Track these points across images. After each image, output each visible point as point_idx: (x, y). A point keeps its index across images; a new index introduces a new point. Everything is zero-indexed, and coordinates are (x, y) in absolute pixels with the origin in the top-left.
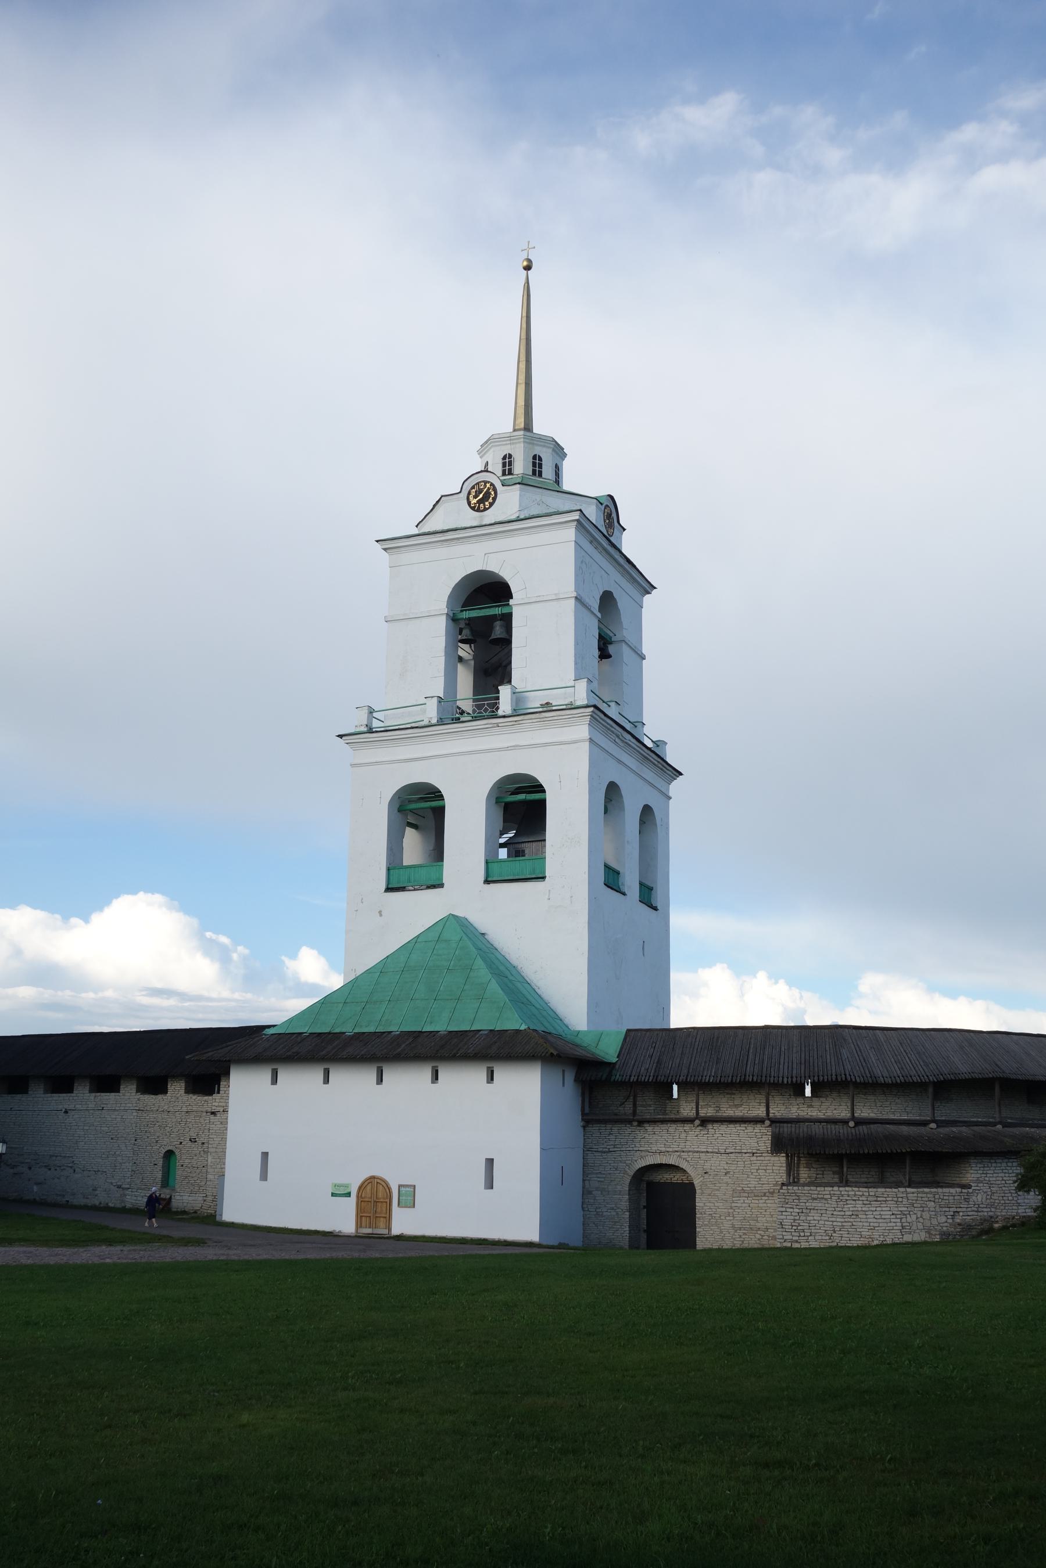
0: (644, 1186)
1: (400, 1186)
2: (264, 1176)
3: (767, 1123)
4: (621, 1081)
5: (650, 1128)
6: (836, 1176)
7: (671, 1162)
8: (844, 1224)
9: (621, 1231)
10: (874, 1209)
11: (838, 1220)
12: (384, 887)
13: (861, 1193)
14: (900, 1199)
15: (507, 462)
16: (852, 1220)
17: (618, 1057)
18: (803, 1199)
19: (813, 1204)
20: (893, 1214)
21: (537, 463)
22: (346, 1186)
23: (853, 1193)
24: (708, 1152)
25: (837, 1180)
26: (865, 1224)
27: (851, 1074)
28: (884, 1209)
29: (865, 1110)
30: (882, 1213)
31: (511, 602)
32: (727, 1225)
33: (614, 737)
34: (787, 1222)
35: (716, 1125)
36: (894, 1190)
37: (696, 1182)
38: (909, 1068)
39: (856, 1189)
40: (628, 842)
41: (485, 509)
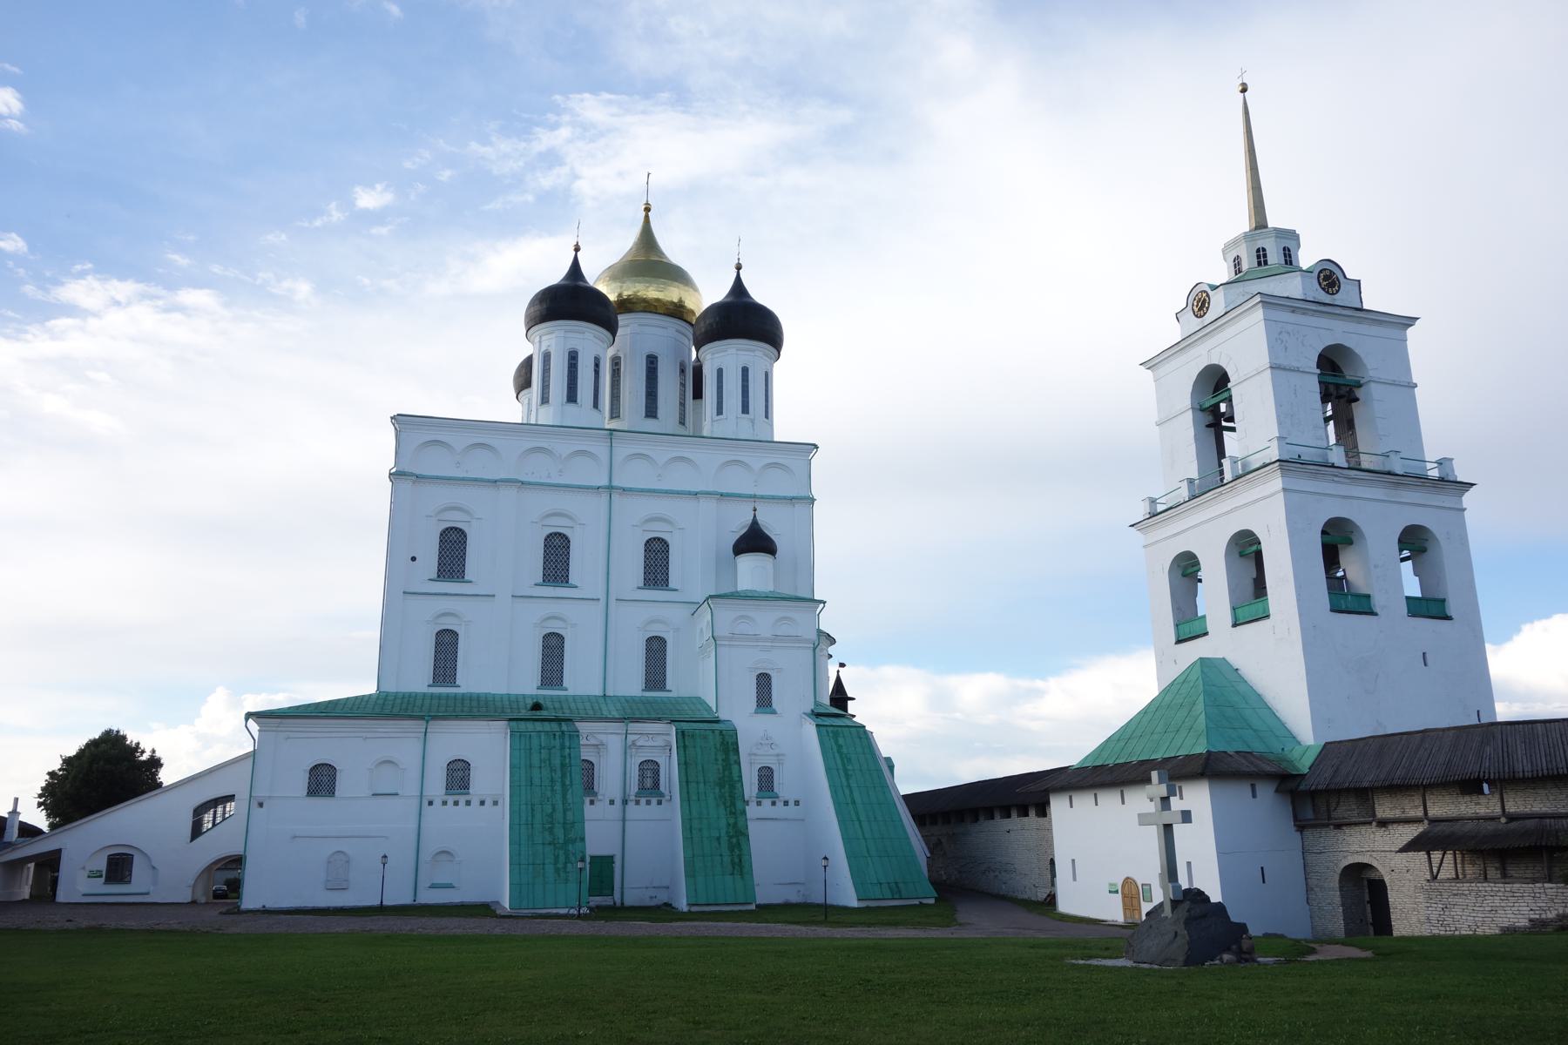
0: (1366, 883)
1: (1142, 885)
2: (1075, 879)
3: (1426, 822)
4: (1445, 782)
5: (1347, 830)
6: (1499, 872)
7: (1365, 861)
8: (1485, 919)
9: (1337, 926)
10: (1512, 905)
11: (1479, 915)
12: (1174, 641)
13: (1497, 889)
14: (1538, 895)
15: (1237, 262)
16: (1492, 916)
17: (1310, 768)
18: (1445, 895)
19: (1457, 900)
20: (1531, 910)
21: (1261, 256)
22: (1115, 885)
23: (1490, 889)
24: (1391, 851)
25: (1499, 876)
26: (1505, 919)
27: (1487, 771)
28: (1521, 904)
29: (1517, 804)
30: (1520, 908)
31: (1230, 385)
32: (1414, 919)
33: (1331, 478)
34: (1433, 917)
35: (1395, 826)
36: (1530, 885)
37: (1387, 879)
38: (1558, 759)
39: (1492, 885)
40: (1376, 566)
41: (1205, 314)
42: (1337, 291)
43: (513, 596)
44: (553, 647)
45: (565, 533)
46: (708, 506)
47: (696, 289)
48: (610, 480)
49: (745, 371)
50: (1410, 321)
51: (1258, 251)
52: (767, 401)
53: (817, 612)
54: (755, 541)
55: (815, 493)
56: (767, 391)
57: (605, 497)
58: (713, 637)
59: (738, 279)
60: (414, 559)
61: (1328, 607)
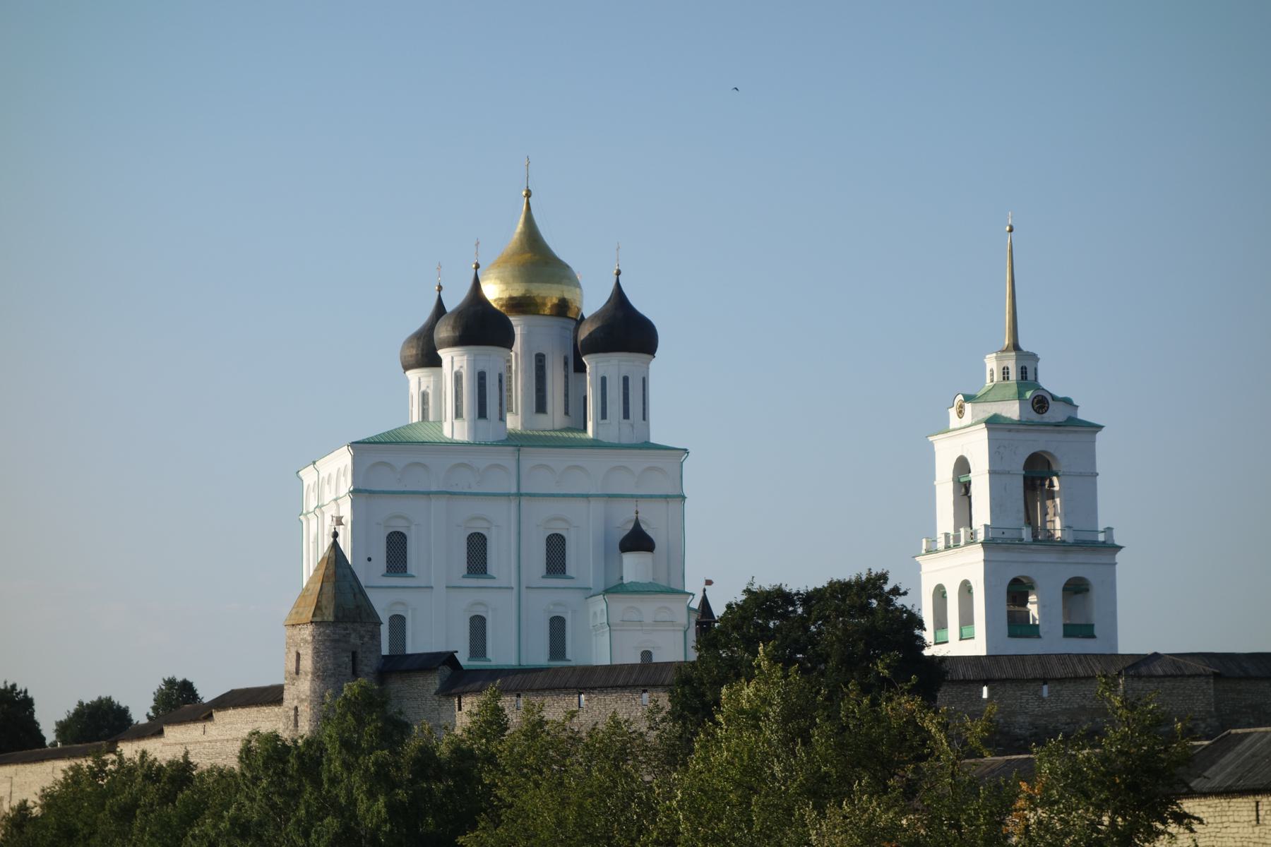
42: (1046, 411)
43: (447, 587)
44: (478, 626)
45: (482, 532)
46: (597, 507)
47: (578, 285)
48: (519, 489)
49: (626, 380)
50: (1100, 427)
51: (1004, 369)
52: (644, 403)
53: (688, 602)
54: (638, 541)
56: (644, 395)
57: (514, 505)
58: (608, 624)
59: (618, 284)
60: (369, 559)
61: (1007, 633)
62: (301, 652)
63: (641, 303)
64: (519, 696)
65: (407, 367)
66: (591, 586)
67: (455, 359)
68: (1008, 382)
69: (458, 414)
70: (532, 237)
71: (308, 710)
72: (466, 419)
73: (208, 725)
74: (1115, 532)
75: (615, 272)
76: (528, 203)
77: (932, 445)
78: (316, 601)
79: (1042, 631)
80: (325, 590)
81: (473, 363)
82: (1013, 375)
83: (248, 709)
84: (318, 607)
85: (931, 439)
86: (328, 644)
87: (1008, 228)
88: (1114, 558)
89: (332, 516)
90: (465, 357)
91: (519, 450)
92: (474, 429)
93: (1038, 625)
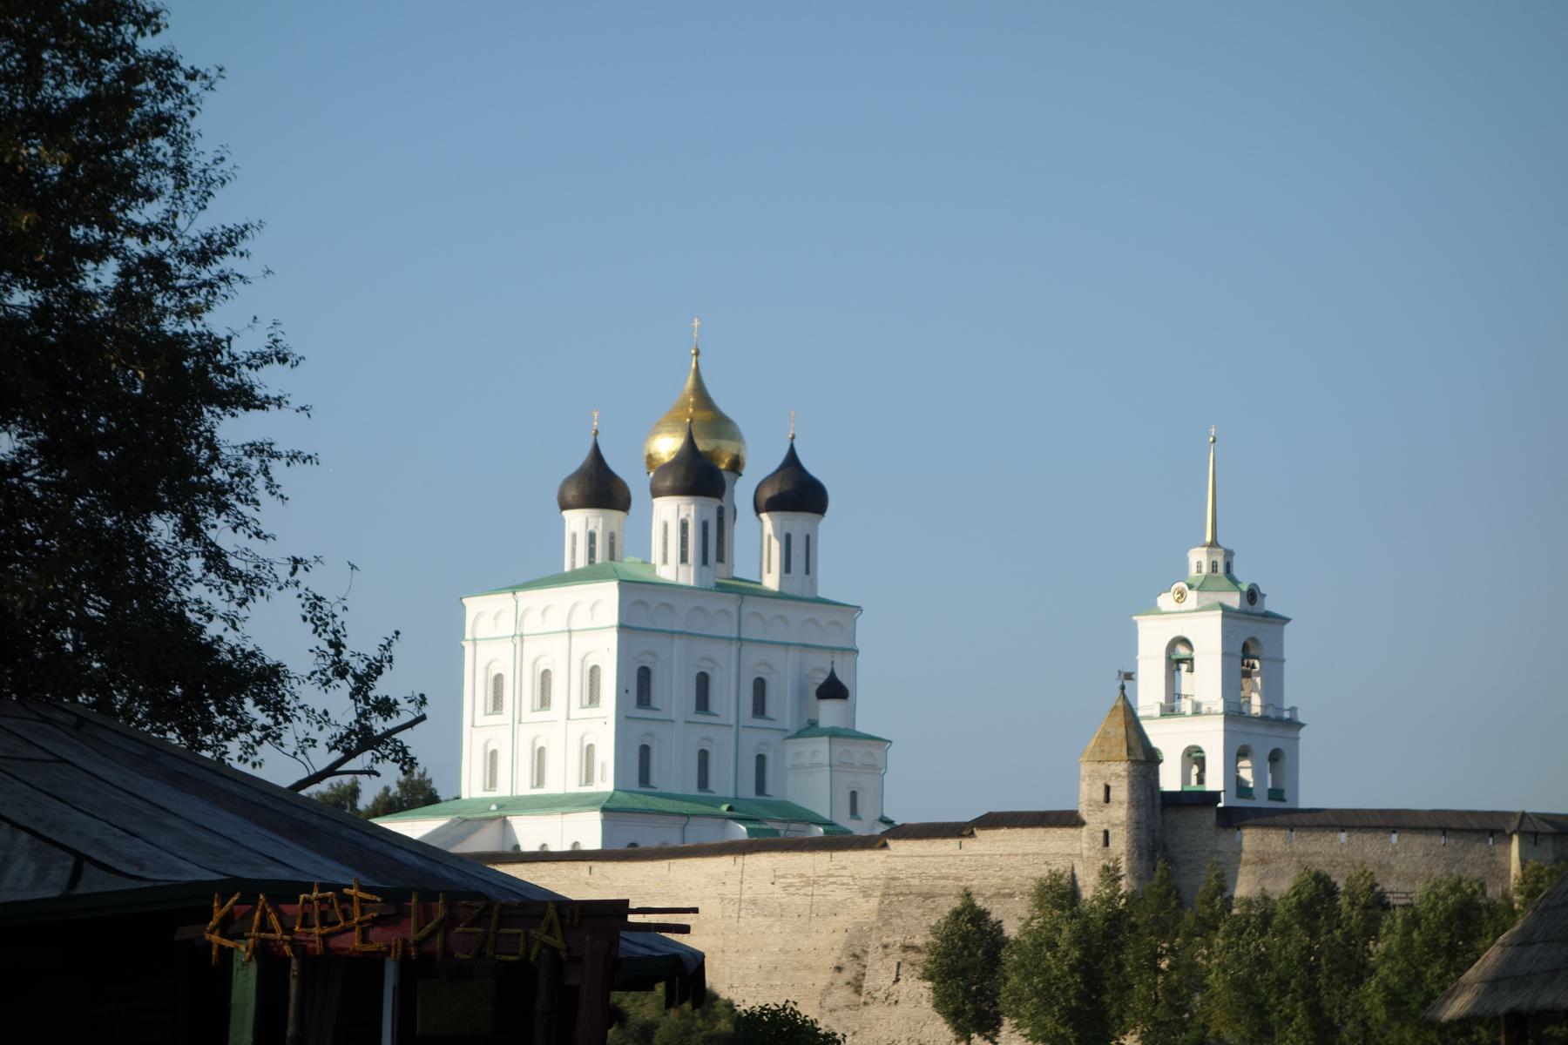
44: (704, 756)
46: (793, 654)
47: (744, 443)
50: (1287, 620)
54: (833, 689)
55: (859, 644)
60: (627, 691)
62: (1111, 784)
63: (813, 465)
64: (1292, 830)
65: (565, 506)
66: (788, 727)
67: (681, 507)
68: (1217, 574)
69: (684, 559)
70: (701, 395)
71: (1125, 833)
72: (693, 564)
73: (966, 842)
74: (1299, 712)
75: (790, 436)
76: (697, 362)
77: (1135, 623)
78: (1125, 743)
79: (1255, 793)
80: (1131, 734)
81: (698, 513)
82: (1221, 569)
83: (1030, 829)
84: (1129, 749)
85: (1135, 618)
86: (1140, 779)
87: (1211, 439)
88: (1298, 734)
89: (1120, 672)
90: (693, 507)
91: (742, 598)
92: (698, 576)
93: (1251, 789)
